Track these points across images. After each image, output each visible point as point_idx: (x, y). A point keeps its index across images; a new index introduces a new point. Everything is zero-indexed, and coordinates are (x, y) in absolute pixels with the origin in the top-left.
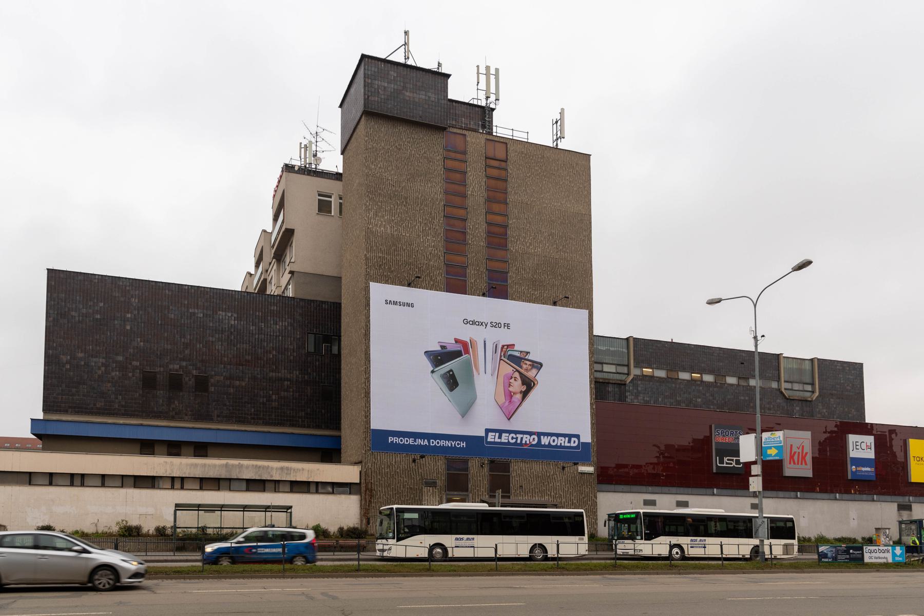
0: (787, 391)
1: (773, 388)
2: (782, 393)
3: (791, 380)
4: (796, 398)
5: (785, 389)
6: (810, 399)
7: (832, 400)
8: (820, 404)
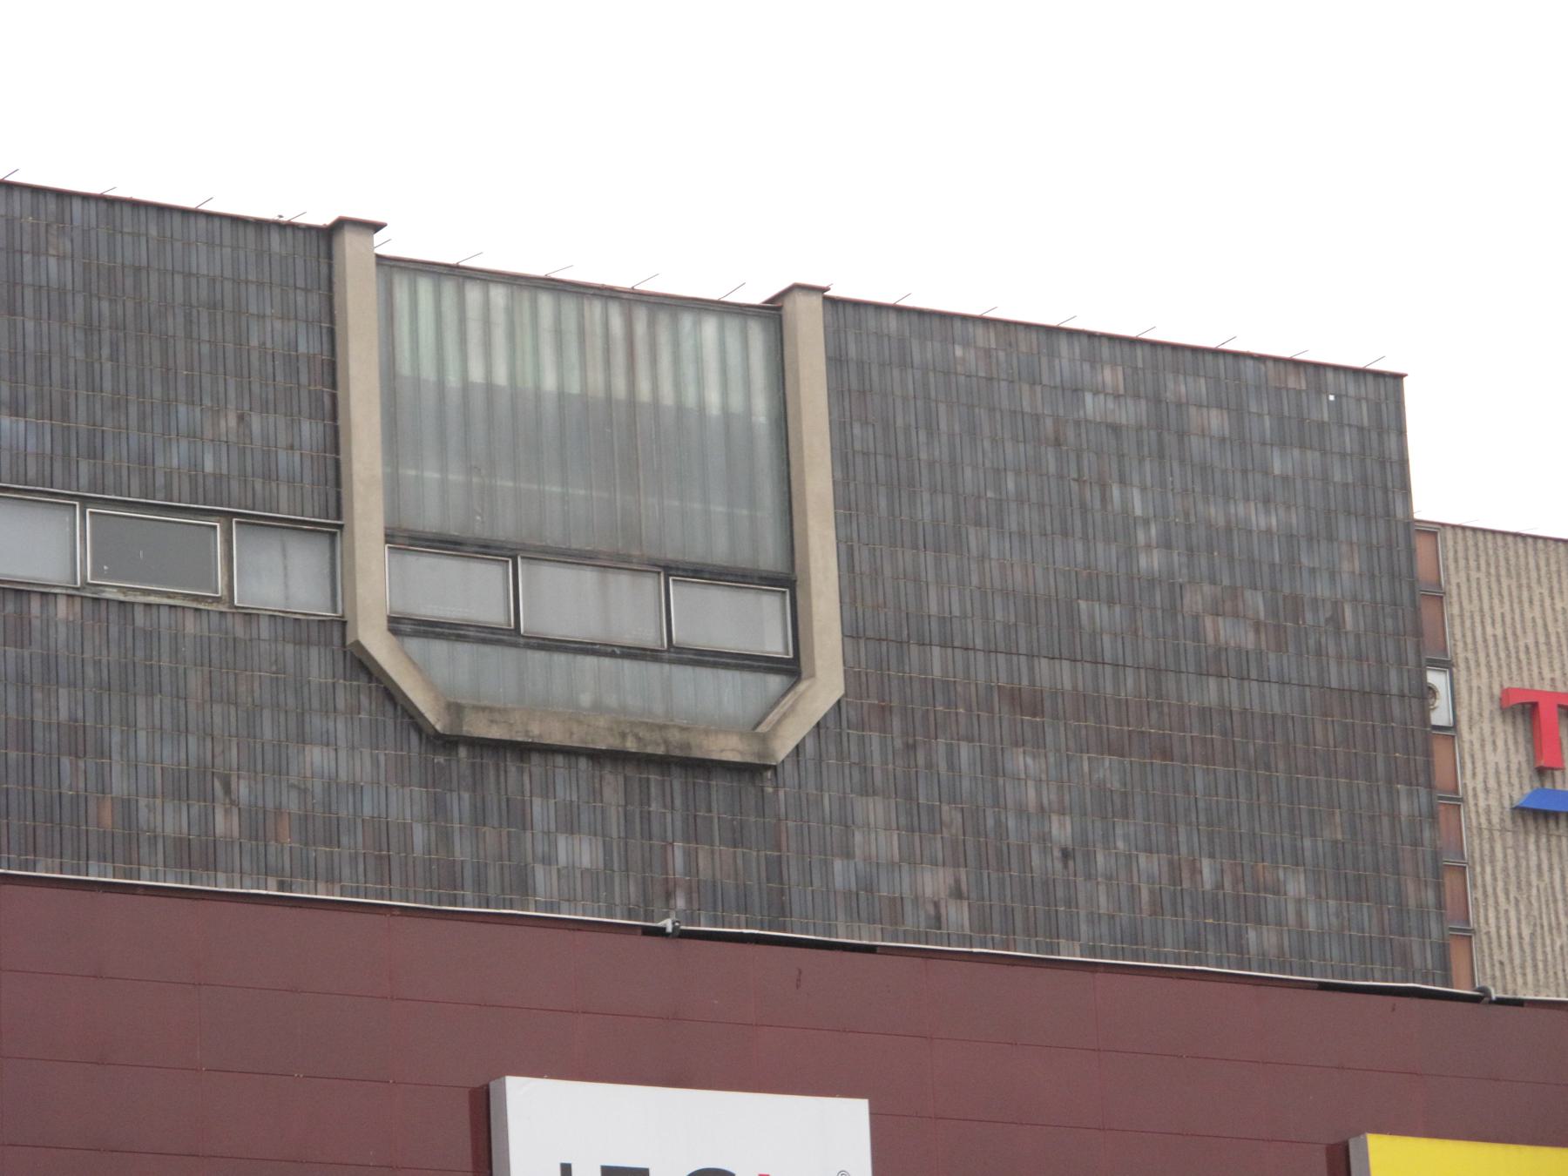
0: (414, 644)
1: (249, 616)
2: (362, 665)
3: (505, 528)
4: (556, 735)
5: (398, 625)
6: (729, 748)
7: (1020, 761)
8: (874, 810)
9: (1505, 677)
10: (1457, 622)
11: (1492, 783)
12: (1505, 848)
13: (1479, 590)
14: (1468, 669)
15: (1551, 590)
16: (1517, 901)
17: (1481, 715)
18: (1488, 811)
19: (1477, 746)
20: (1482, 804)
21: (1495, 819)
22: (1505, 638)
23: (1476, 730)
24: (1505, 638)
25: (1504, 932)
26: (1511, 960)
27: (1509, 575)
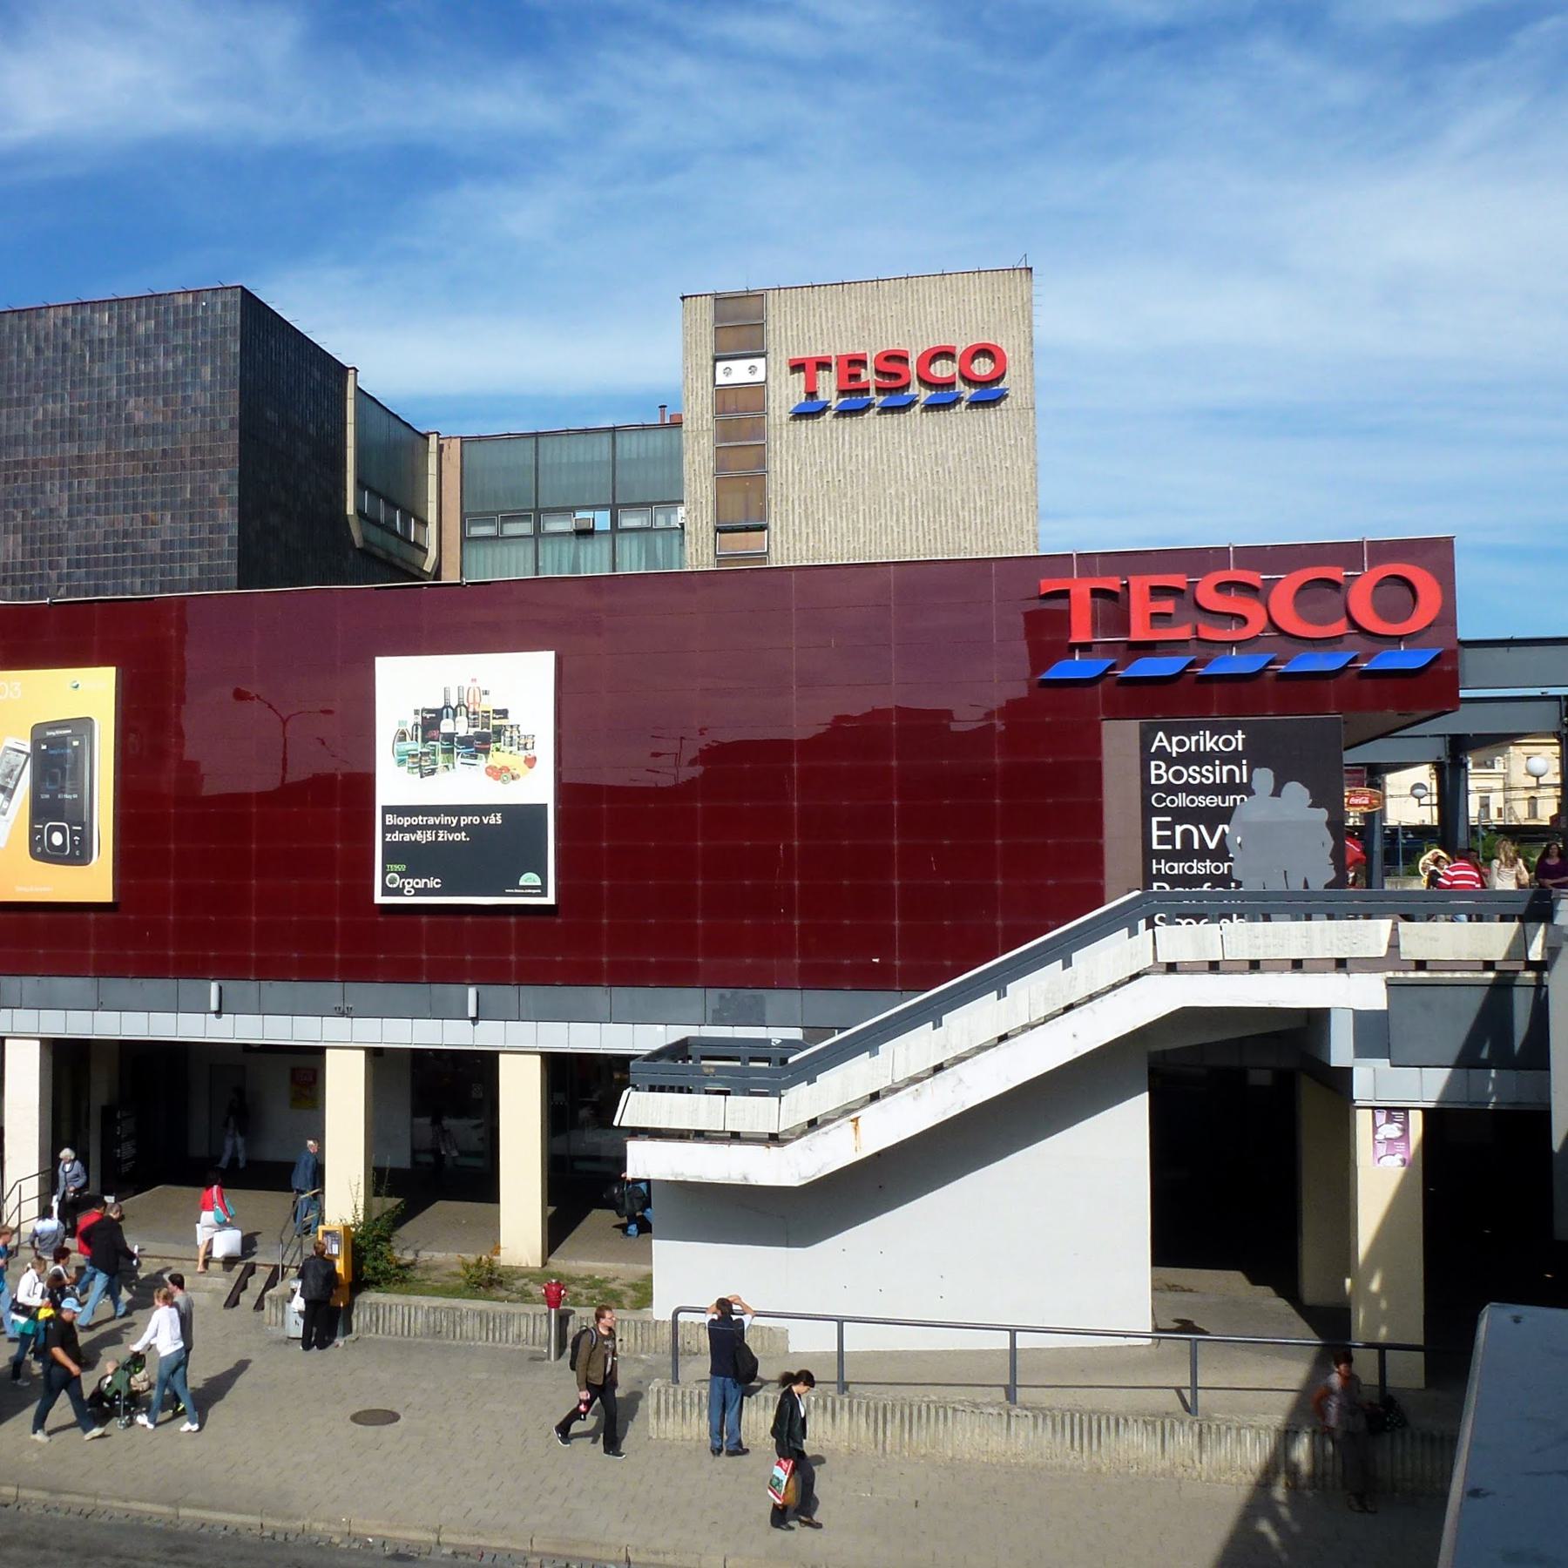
9: (796, 351)
10: (771, 332)
11: (784, 402)
12: (788, 431)
13: (785, 315)
14: (776, 353)
15: (826, 310)
16: (793, 455)
17: (780, 373)
18: (780, 417)
19: (777, 387)
20: (778, 414)
21: (784, 419)
22: (798, 335)
23: (777, 382)
24: (798, 335)
25: (784, 470)
26: (787, 481)
27: (803, 306)
